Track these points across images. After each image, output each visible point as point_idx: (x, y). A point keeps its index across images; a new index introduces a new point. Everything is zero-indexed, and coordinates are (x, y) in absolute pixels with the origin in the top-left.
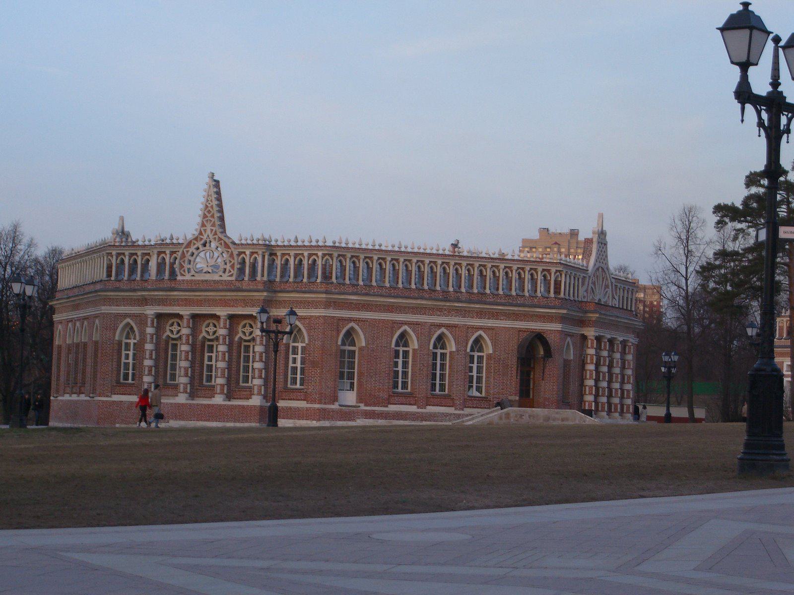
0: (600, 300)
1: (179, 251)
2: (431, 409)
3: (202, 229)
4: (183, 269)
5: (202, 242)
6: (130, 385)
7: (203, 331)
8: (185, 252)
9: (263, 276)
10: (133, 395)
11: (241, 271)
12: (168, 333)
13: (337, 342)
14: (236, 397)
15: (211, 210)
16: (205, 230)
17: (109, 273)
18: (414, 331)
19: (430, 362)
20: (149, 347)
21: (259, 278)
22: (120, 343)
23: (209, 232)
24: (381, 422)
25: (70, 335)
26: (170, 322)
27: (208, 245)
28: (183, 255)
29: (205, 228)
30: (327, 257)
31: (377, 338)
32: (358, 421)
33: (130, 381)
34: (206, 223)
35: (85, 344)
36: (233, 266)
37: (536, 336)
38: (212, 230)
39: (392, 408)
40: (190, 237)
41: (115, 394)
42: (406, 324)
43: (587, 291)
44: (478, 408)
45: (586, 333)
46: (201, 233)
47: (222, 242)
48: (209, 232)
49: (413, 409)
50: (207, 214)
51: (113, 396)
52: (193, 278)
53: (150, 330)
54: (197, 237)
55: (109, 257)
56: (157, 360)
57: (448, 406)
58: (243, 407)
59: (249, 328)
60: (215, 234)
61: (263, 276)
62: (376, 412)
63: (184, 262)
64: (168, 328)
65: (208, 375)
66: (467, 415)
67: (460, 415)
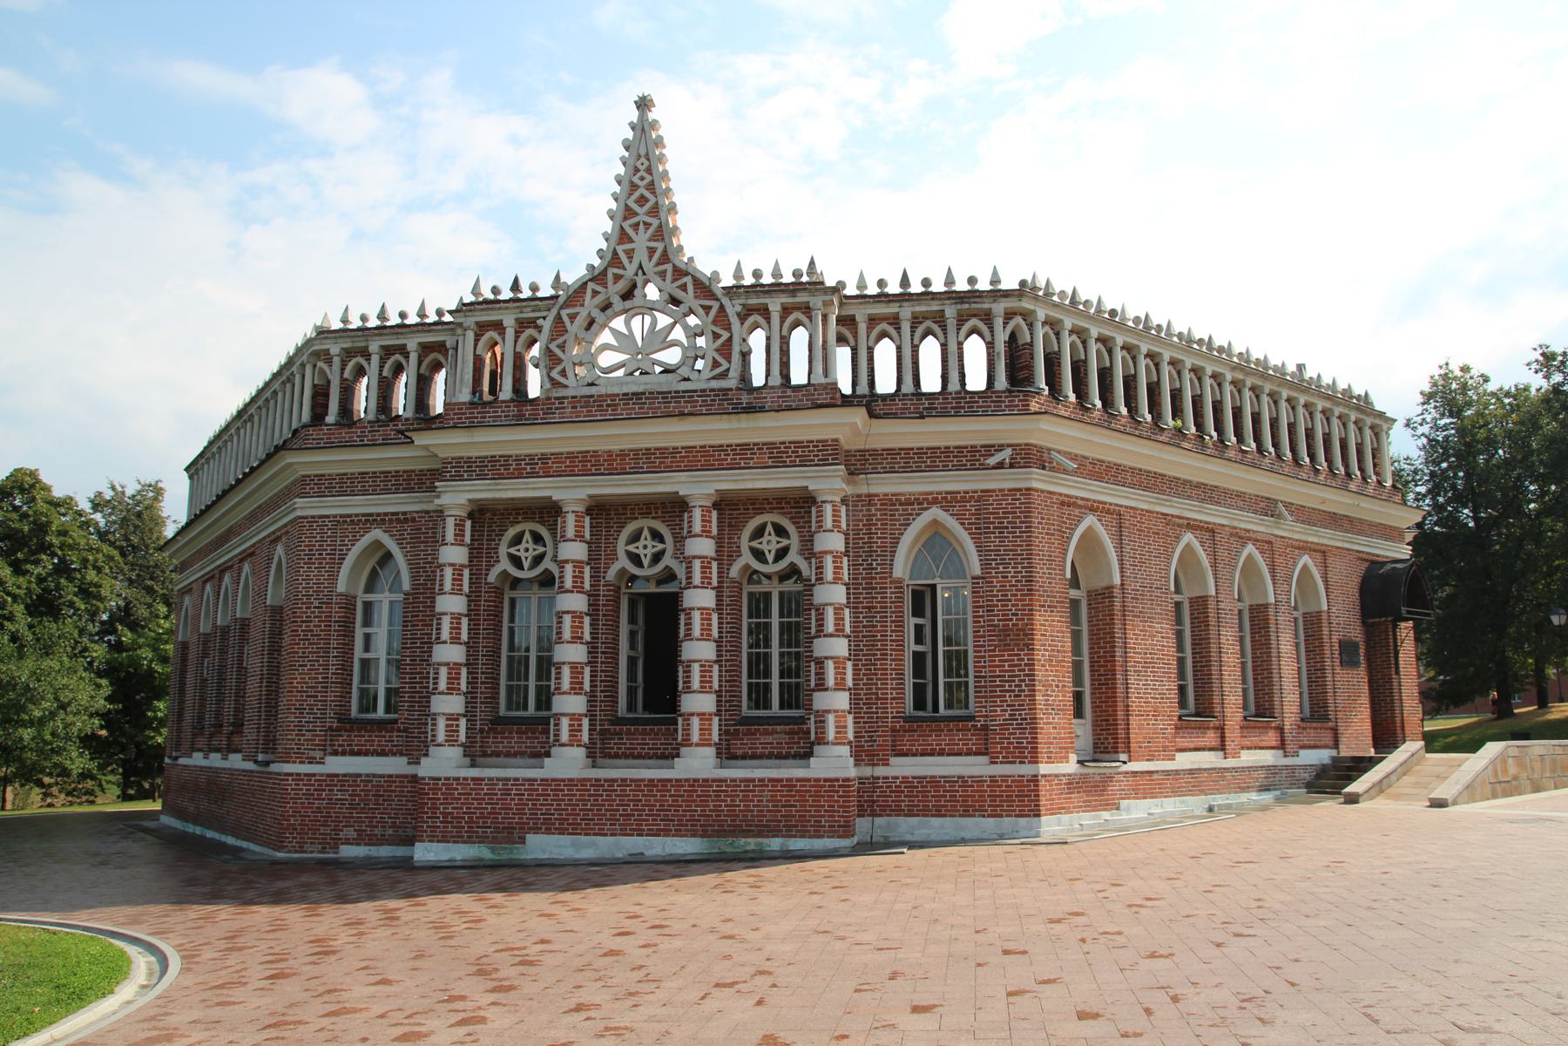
1: (544, 318)
3: (620, 249)
4: (559, 368)
5: (622, 286)
6: (381, 724)
8: (566, 319)
10: (394, 754)
12: (505, 565)
14: (739, 752)
15: (647, 194)
17: (319, 411)
20: (451, 604)
22: (349, 603)
23: (641, 255)
25: (207, 613)
26: (511, 532)
29: (628, 246)
30: (1019, 320)
33: (381, 712)
35: (244, 625)
38: (652, 251)
40: (572, 277)
41: (335, 753)
46: (615, 260)
47: (688, 279)
48: (641, 255)
51: (329, 759)
53: (454, 554)
54: (604, 273)
55: (320, 364)
56: (471, 646)
58: (789, 783)
64: (503, 550)
65: (948, 651)
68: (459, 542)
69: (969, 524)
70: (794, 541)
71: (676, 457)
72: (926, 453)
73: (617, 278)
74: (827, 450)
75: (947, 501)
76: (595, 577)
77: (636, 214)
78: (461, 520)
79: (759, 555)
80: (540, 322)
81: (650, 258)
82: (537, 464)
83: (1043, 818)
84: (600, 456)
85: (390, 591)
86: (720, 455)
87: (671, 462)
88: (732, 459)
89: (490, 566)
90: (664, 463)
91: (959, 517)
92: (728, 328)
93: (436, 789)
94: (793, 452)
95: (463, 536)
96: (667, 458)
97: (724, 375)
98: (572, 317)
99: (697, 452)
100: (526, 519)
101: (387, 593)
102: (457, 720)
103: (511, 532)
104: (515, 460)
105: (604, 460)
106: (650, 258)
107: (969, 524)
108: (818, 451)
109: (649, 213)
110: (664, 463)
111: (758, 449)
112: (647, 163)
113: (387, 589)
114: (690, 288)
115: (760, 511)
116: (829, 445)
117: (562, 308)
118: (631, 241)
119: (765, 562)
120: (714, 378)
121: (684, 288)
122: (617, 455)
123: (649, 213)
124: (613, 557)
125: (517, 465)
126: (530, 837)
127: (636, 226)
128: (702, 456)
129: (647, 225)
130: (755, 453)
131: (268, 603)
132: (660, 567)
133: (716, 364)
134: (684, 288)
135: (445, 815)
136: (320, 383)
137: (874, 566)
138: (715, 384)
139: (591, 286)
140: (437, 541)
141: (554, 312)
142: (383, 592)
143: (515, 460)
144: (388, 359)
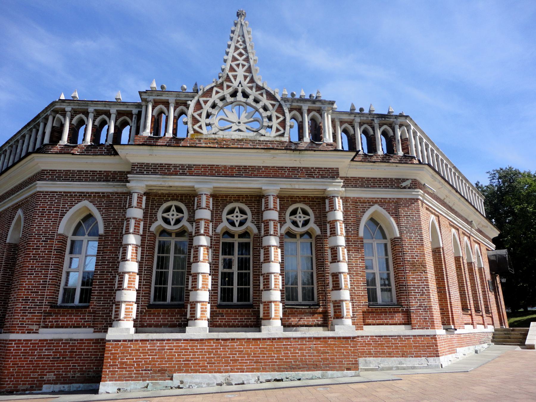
1: (191, 101)
5: (231, 90)
8: (202, 102)
10: (85, 327)
12: (160, 222)
15: (243, 52)
16: (235, 77)
22: (63, 240)
23: (240, 78)
26: (165, 206)
28: (198, 106)
29: (234, 73)
38: (246, 77)
41: (46, 327)
48: (240, 78)
51: (41, 330)
63: (200, 115)
64: (160, 214)
68: (139, 206)
69: (392, 213)
70: (312, 217)
71: (259, 171)
72: (371, 180)
73: (228, 87)
74: (334, 173)
75: (382, 202)
76: (215, 227)
77: (237, 60)
78: (140, 195)
79: (295, 223)
80: (189, 102)
81: (245, 80)
82: (186, 169)
83: (440, 358)
84: (220, 168)
86: (282, 172)
87: (257, 173)
88: (288, 174)
89: (151, 223)
90: (253, 173)
91: (387, 210)
94: (317, 172)
95: (141, 204)
96: (255, 171)
97: (282, 135)
98: (206, 102)
99: (270, 169)
100: (173, 200)
101: (86, 236)
102: (132, 305)
103: (165, 206)
104: (174, 167)
105: (222, 170)
106: (245, 80)
107: (392, 213)
108: (330, 173)
109: (244, 60)
110: (253, 173)
111: (301, 170)
112: (243, 39)
113: (87, 234)
115: (295, 202)
116: (335, 171)
119: (297, 226)
120: (277, 136)
121: (261, 94)
122: (229, 168)
123: (244, 60)
125: (174, 169)
127: (238, 65)
128: (273, 171)
129: (243, 66)
130: (299, 172)
131: (8, 241)
132: (243, 228)
133: (278, 130)
135: (122, 363)
136: (56, 126)
137: (350, 230)
138: (278, 139)
139: (215, 89)
141: (196, 98)
142: (84, 235)
143: (174, 167)
144: (98, 117)
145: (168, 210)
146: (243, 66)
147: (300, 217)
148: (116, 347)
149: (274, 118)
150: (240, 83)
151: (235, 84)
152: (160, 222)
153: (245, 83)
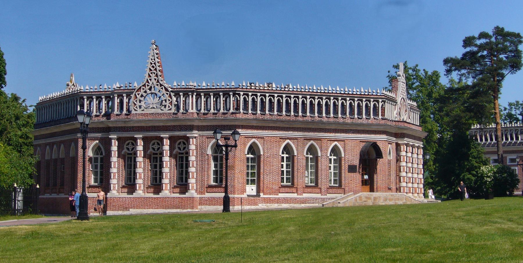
0: (403, 119)
2: (305, 195)
4: (136, 106)
5: (149, 87)
7: (151, 148)
9: (192, 109)
11: (178, 107)
12: (125, 150)
13: (244, 152)
14: (175, 192)
16: (151, 80)
18: (293, 143)
19: (304, 164)
21: (190, 110)
23: (153, 80)
24: (275, 206)
27: (153, 89)
29: (150, 78)
31: (270, 149)
32: (260, 205)
34: (151, 75)
35: (62, 160)
36: (171, 103)
37: (372, 145)
39: (281, 195)
42: (288, 139)
43: (397, 114)
44: (336, 193)
45: (399, 142)
49: (295, 195)
50: (152, 68)
52: (143, 112)
55: (81, 100)
57: (316, 193)
59: (131, 147)
60: (158, 81)
61: (192, 109)
62: (271, 199)
63: (136, 101)
66: (329, 199)
67: (324, 199)
73: (148, 85)
80: (131, 95)
83: (235, 206)
85: (100, 155)
89: (122, 150)
92: (171, 98)
93: (111, 200)
98: (138, 94)
100: (130, 140)
101: (99, 155)
114: (164, 88)
117: (136, 92)
118: (151, 77)
120: (168, 110)
121: (162, 88)
124: (149, 148)
126: (130, 210)
129: (154, 73)
134: (162, 88)
135: (113, 205)
140: (110, 145)
145: (128, 144)
146: (154, 73)
147: (182, 146)
148: (111, 200)
149: (167, 101)
150: (153, 83)
151: (150, 84)
152: (125, 150)
153: (155, 82)
